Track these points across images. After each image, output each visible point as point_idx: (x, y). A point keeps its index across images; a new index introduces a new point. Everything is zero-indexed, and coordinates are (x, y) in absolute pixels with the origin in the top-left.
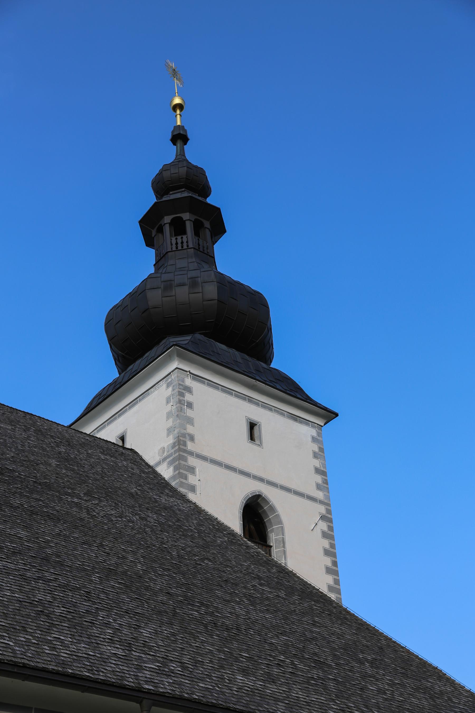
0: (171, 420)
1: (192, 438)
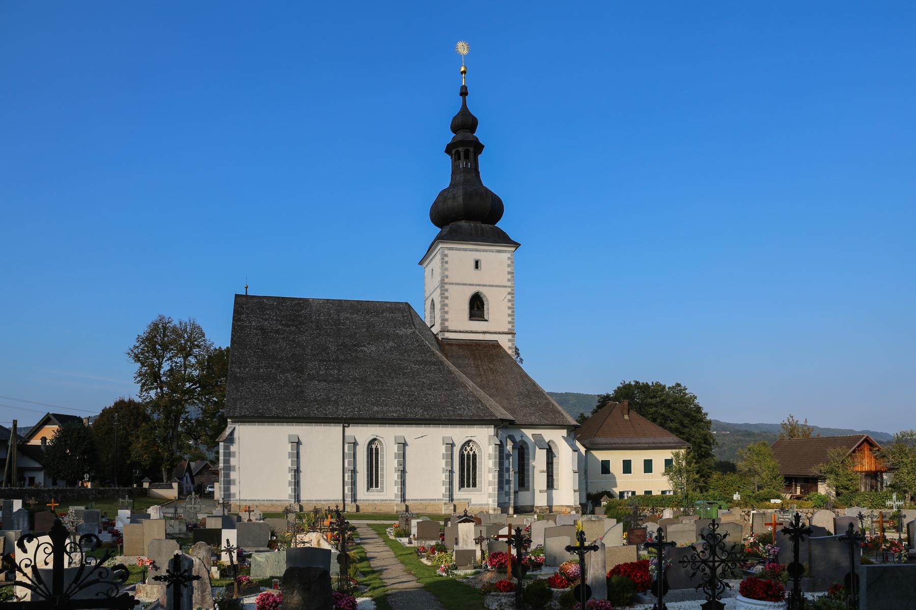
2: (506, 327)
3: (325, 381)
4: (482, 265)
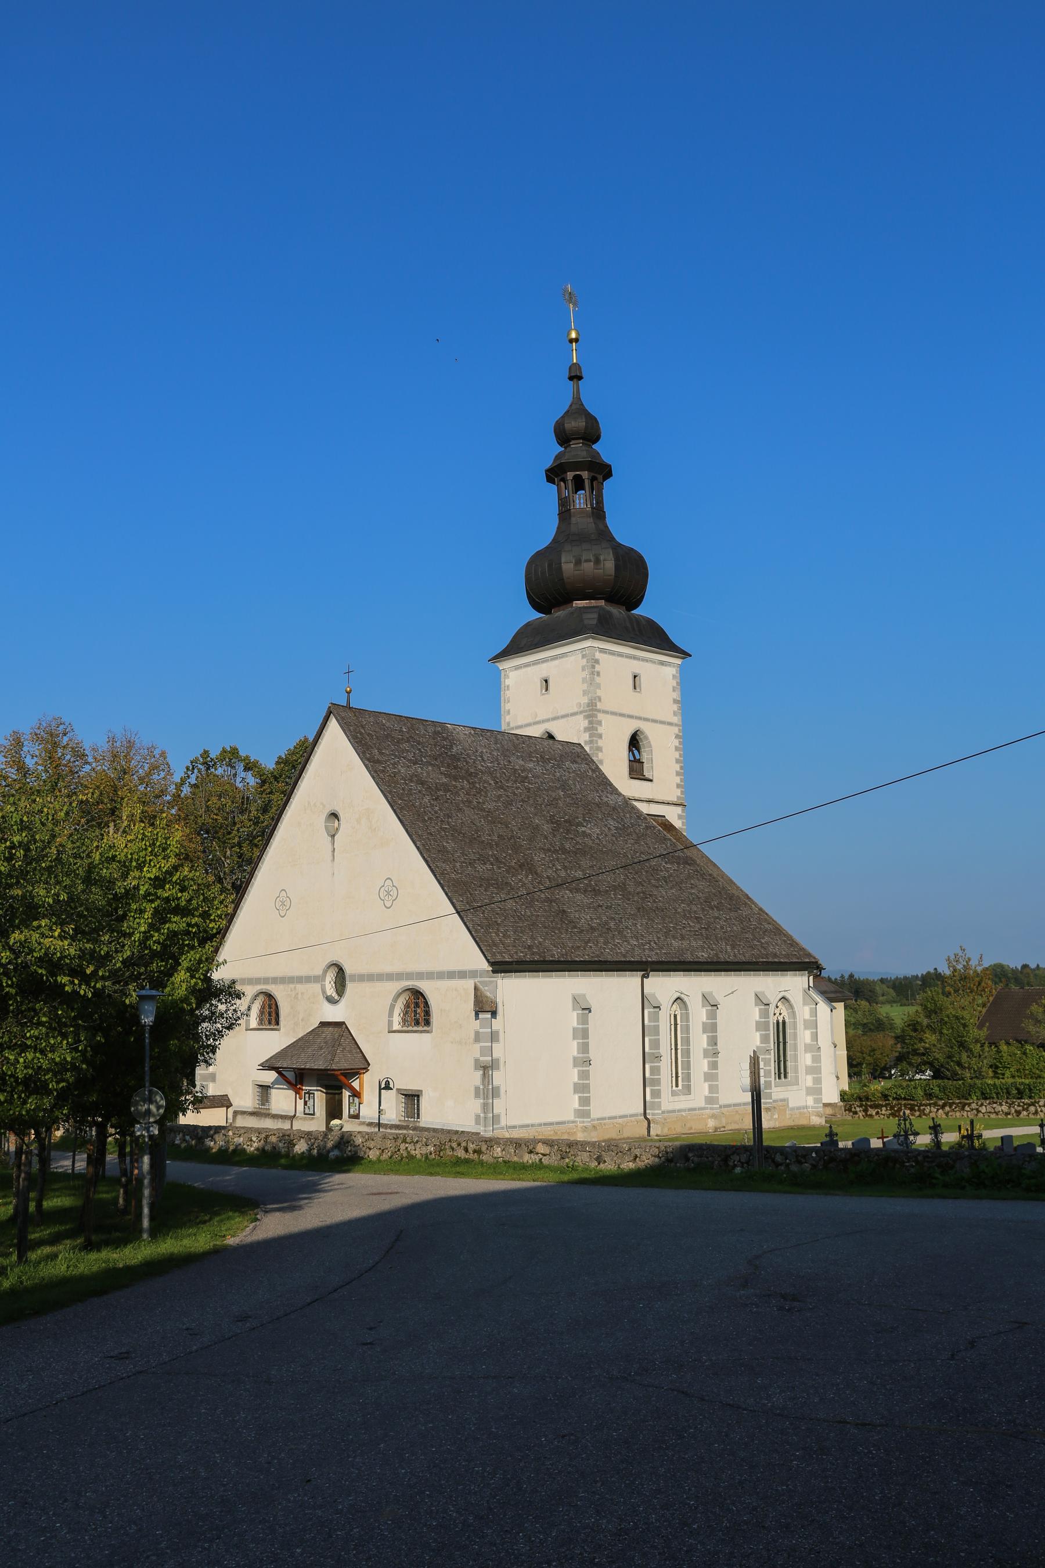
0: (586, 685)
1: (600, 700)
2: (674, 795)
3: (578, 890)
4: (643, 681)
